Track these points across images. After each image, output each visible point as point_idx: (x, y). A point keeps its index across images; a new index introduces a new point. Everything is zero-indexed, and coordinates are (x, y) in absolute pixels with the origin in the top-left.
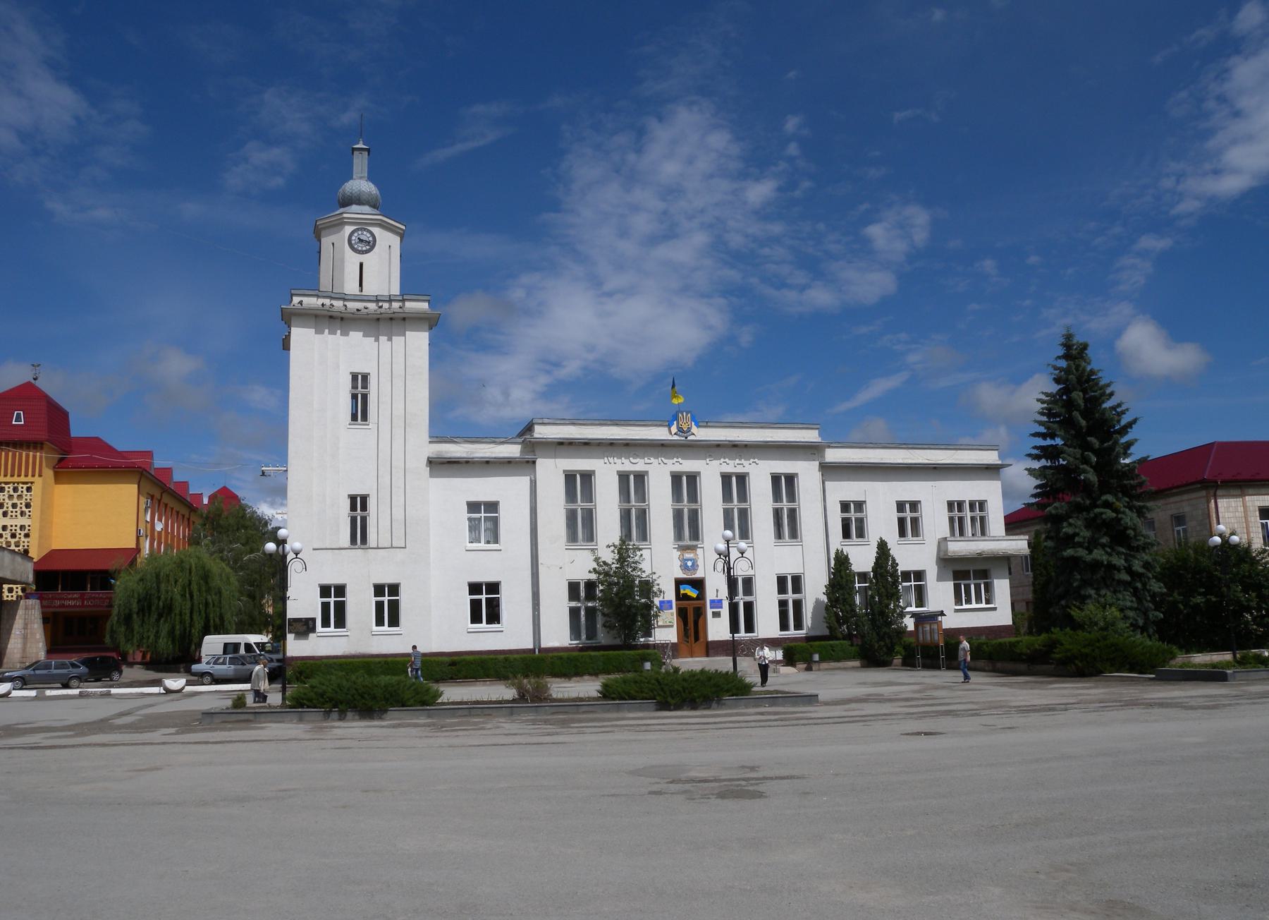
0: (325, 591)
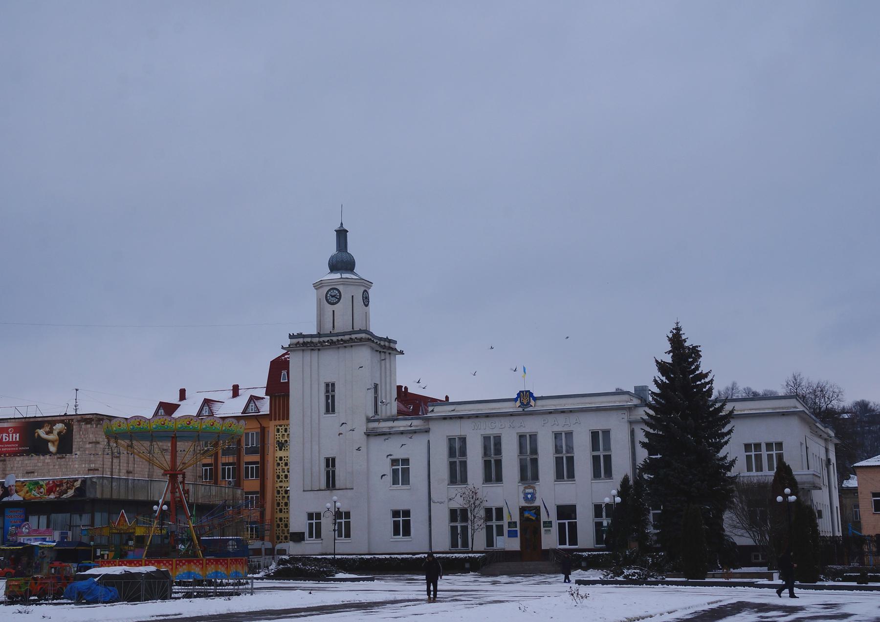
0: (310, 516)
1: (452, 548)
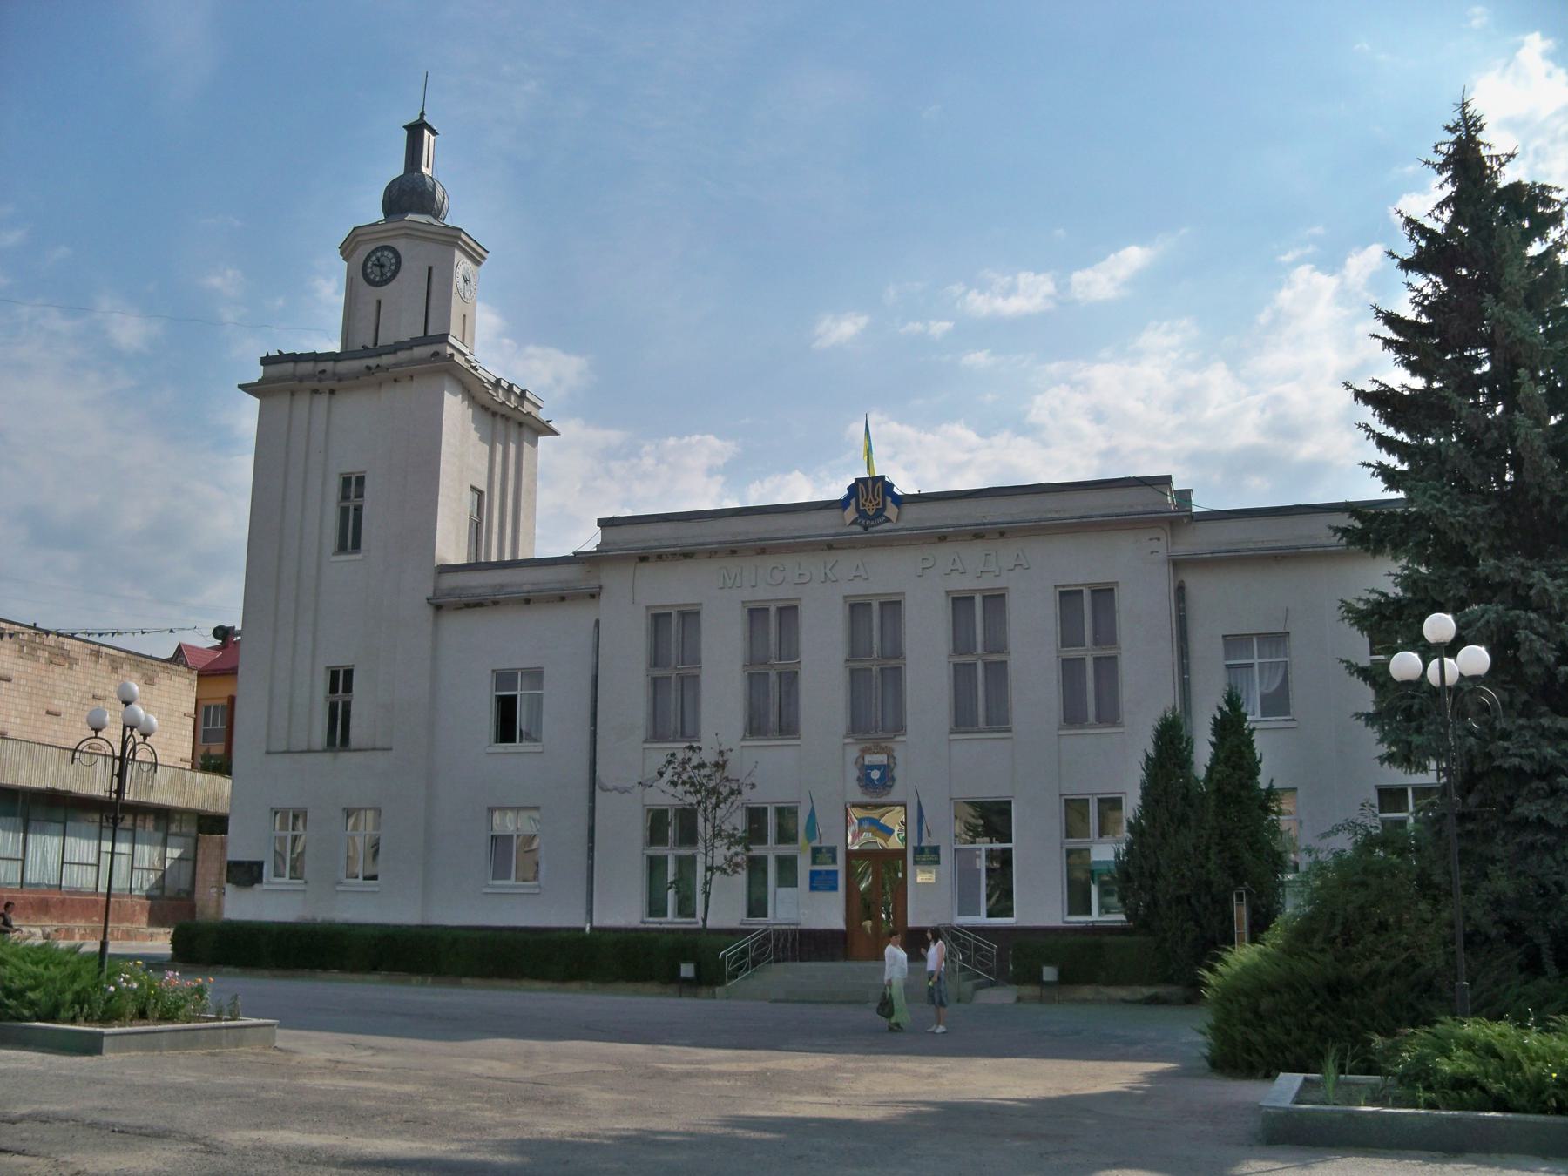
1: (650, 916)
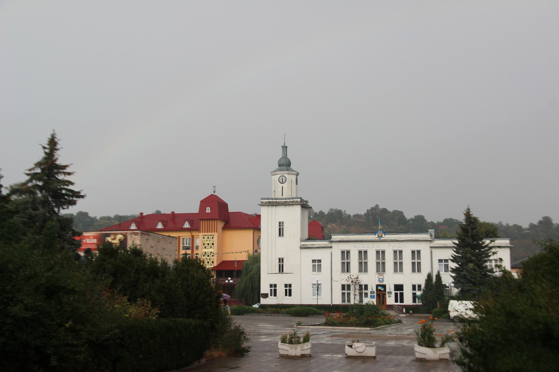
0: (271, 286)
